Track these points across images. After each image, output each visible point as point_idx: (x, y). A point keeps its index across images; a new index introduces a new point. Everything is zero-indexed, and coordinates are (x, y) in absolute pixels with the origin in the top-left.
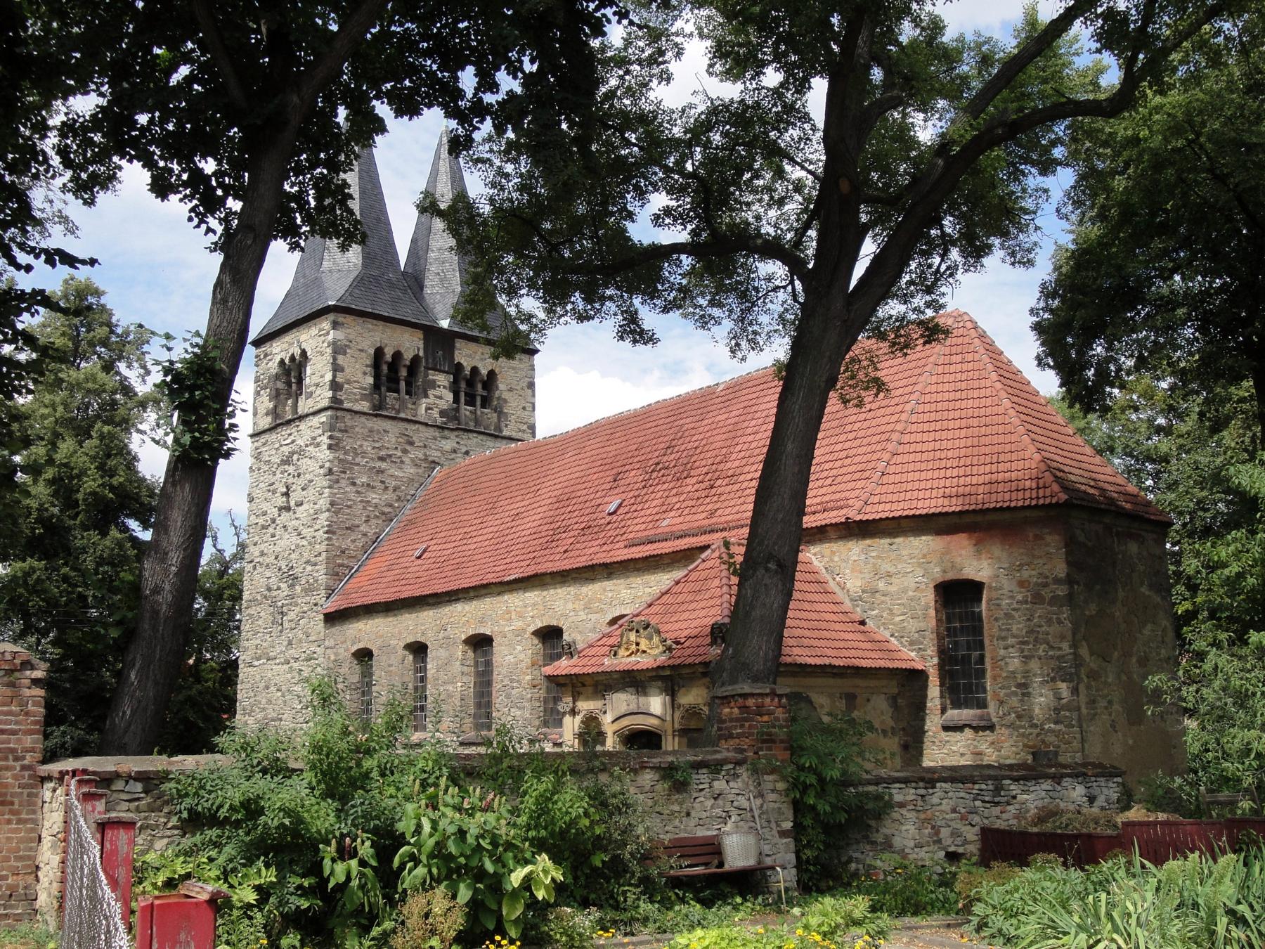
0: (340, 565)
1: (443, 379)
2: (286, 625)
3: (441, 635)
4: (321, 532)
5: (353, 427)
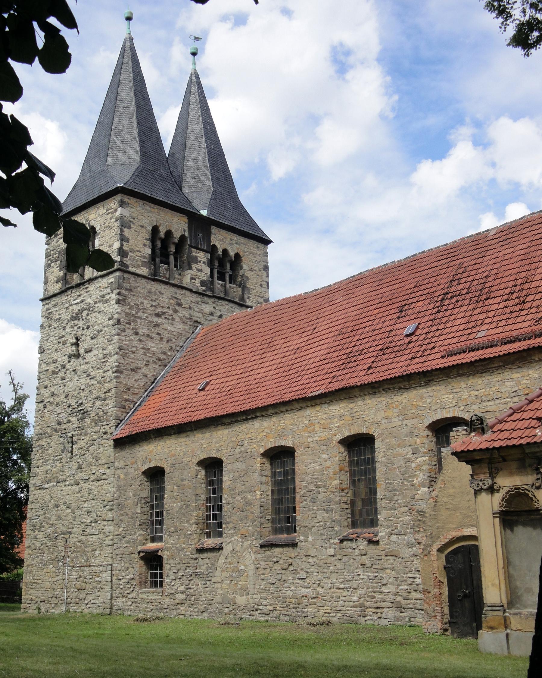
0: (126, 400)
1: (203, 256)
2: (75, 452)
3: (238, 450)
4: (110, 372)
5: (136, 287)
